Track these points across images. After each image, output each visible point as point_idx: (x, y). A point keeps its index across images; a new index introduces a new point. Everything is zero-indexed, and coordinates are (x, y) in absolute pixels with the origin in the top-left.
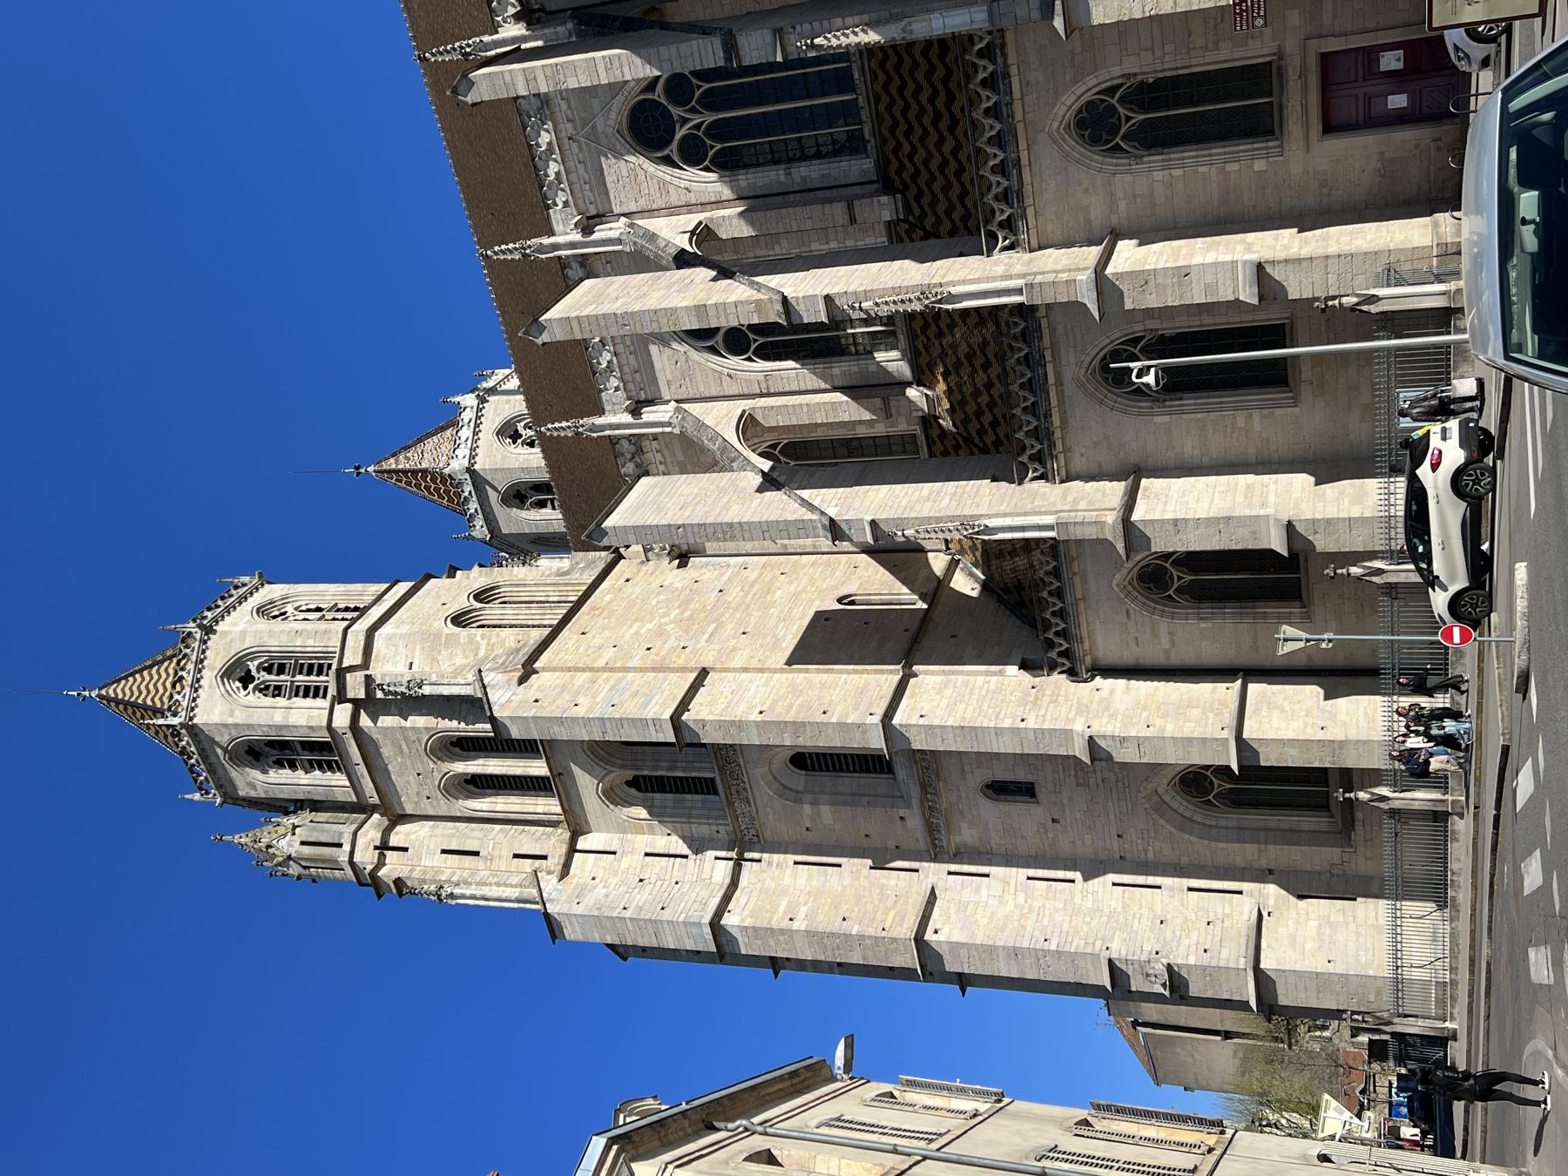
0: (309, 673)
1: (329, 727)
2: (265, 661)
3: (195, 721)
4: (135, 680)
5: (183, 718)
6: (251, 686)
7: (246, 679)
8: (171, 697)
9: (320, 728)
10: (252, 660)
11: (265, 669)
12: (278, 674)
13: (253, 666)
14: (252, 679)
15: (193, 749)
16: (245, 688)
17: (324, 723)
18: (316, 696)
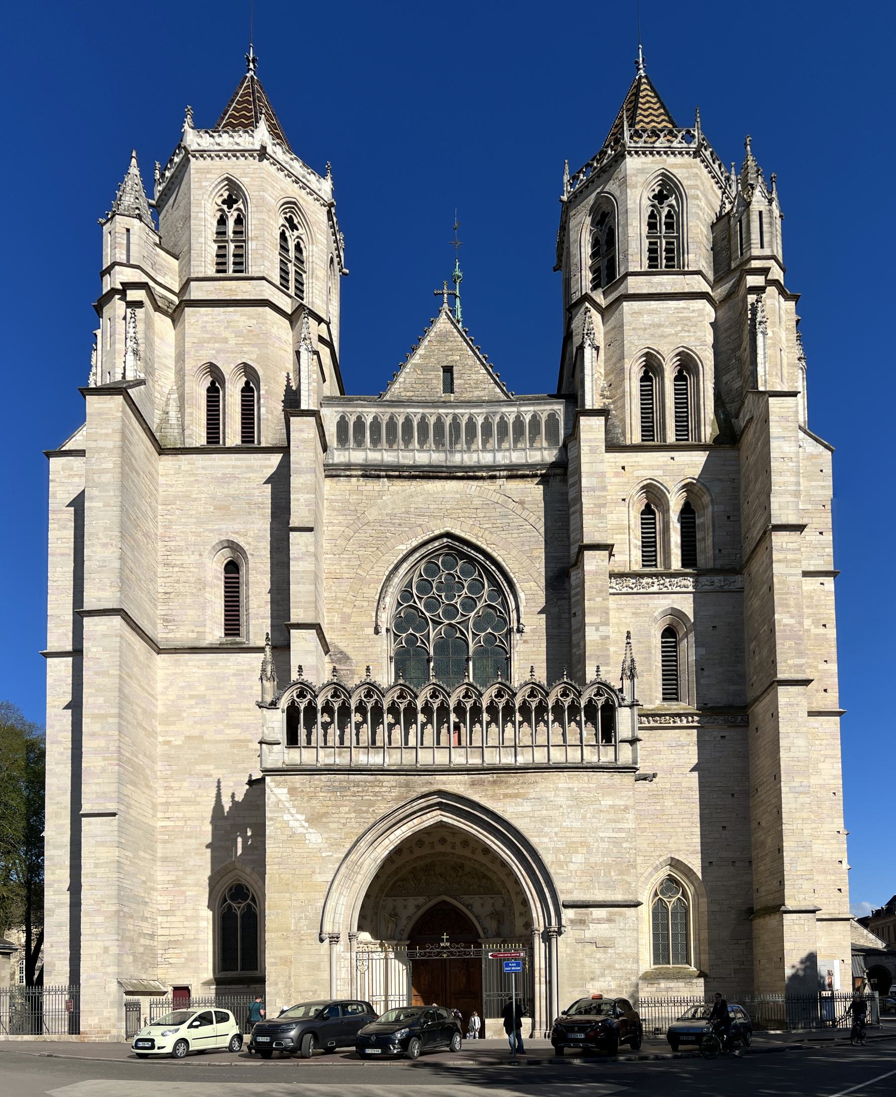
0: (667, 250)
1: (628, 274)
2: (675, 211)
3: (628, 159)
4: (655, 104)
5: (629, 145)
6: (656, 202)
7: (660, 197)
8: (644, 131)
9: (627, 268)
10: (676, 199)
11: (669, 212)
12: (665, 223)
13: (672, 200)
14: (661, 203)
15: (605, 161)
16: (655, 197)
17: (631, 269)
18: (650, 259)
